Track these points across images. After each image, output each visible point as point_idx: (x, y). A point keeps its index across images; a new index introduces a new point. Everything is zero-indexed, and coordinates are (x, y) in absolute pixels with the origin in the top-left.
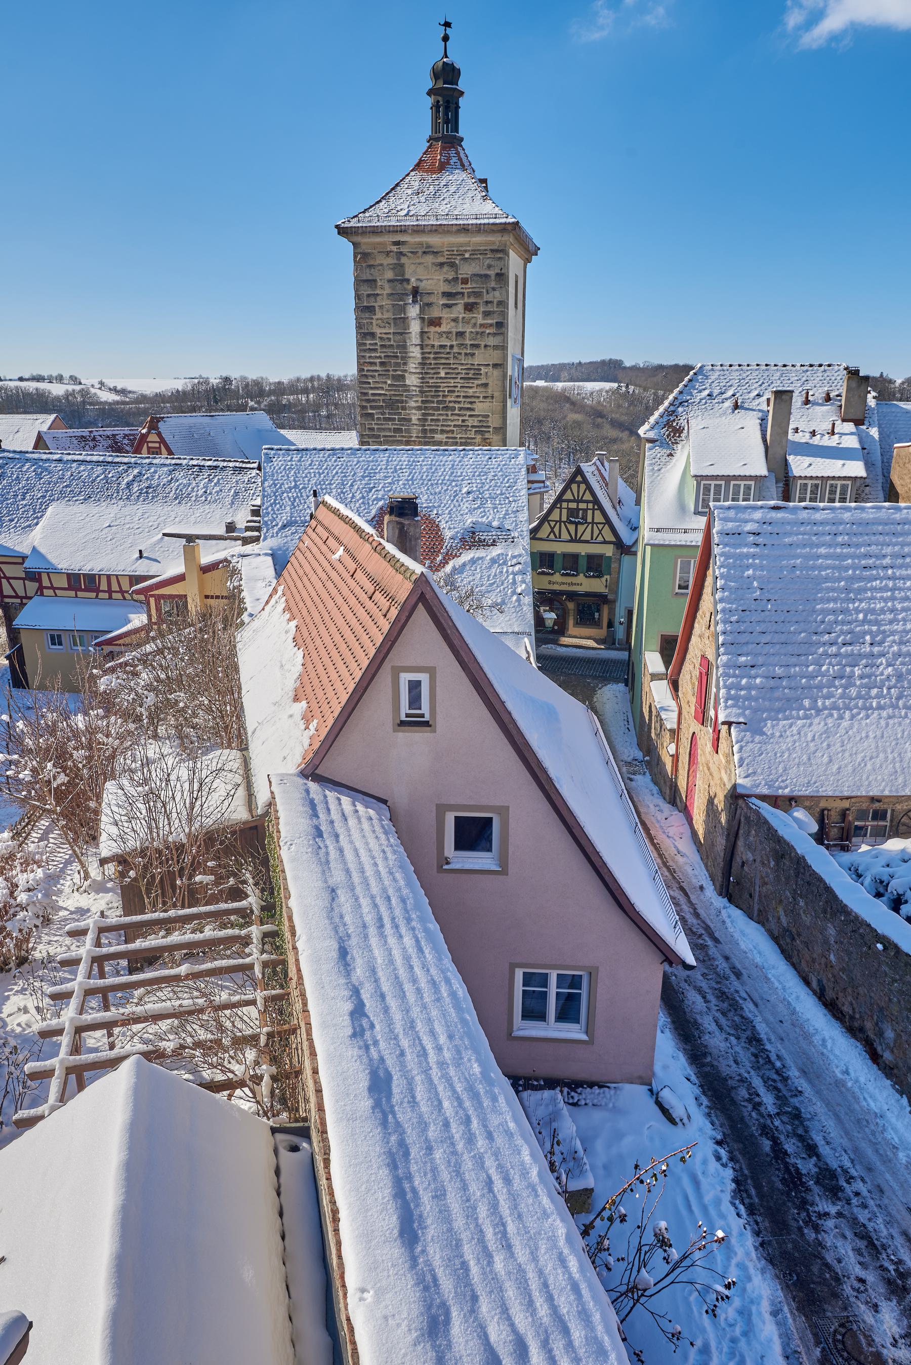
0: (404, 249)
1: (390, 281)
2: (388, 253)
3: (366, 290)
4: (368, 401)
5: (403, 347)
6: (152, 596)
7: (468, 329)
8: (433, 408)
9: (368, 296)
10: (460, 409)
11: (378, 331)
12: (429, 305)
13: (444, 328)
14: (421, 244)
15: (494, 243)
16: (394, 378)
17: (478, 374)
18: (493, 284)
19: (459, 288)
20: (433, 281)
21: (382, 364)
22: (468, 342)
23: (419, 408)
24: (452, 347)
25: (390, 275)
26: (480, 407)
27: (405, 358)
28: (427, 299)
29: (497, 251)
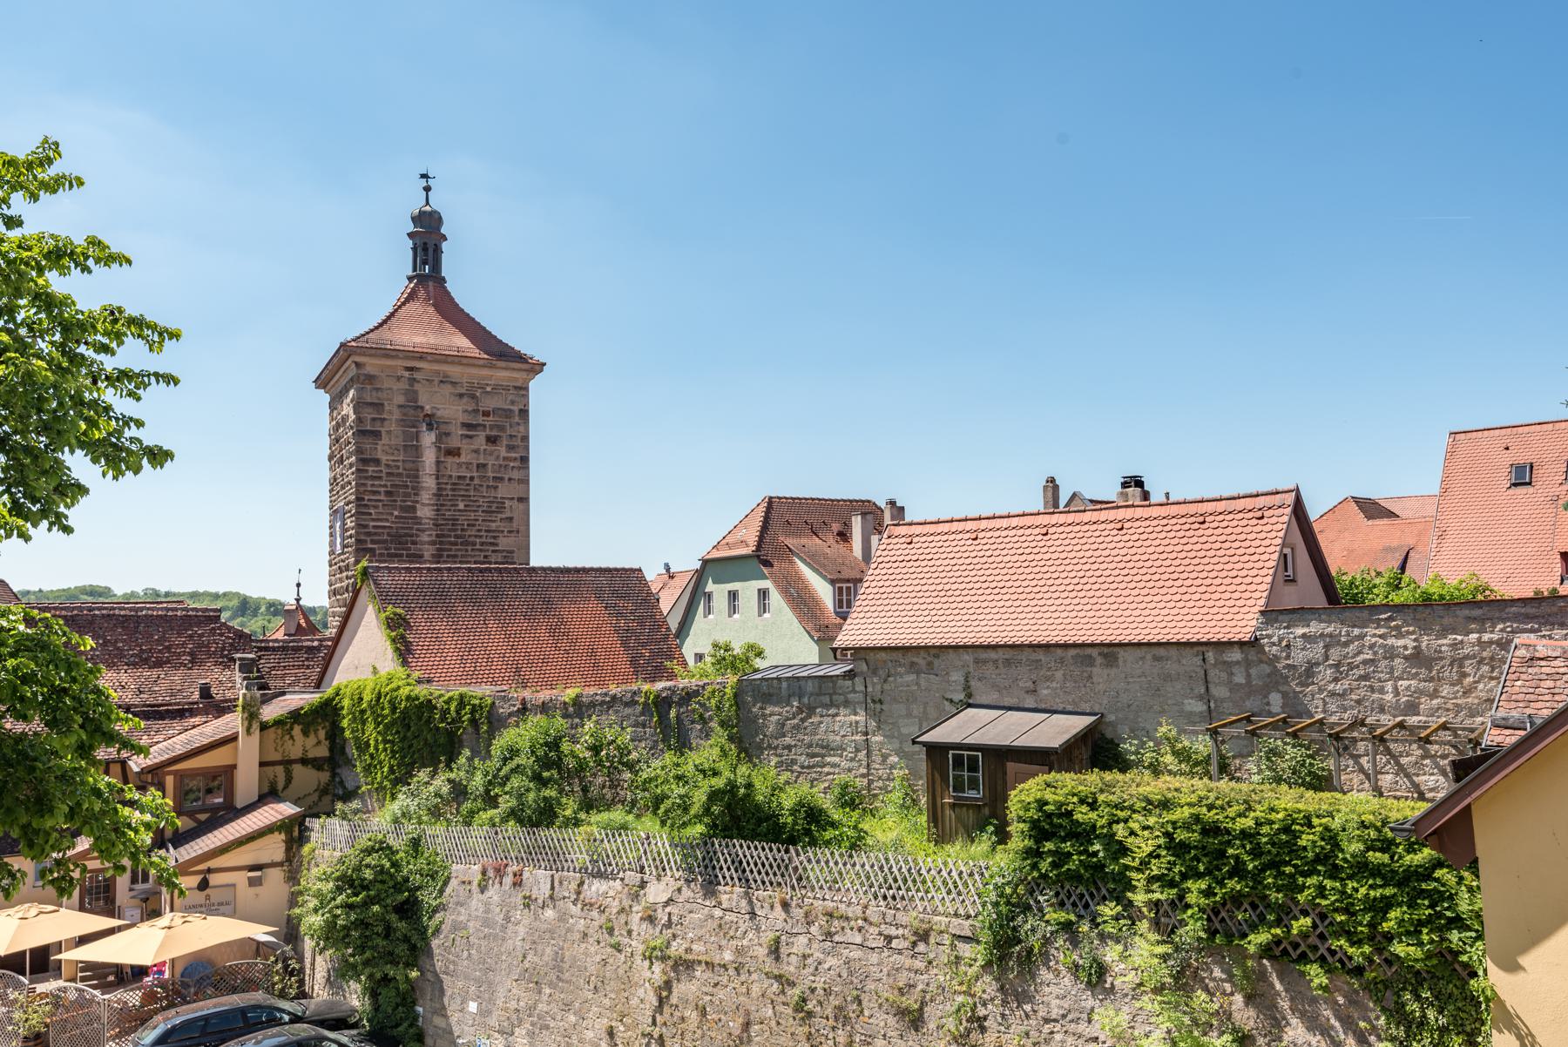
0: (417, 375)
1: (400, 406)
2: (399, 378)
3: (369, 414)
4: (369, 534)
5: (415, 476)
6: (170, 773)
7: (491, 462)
8: (452, 543)
9: (374, 419)
10: (482, 544)
11: (384, 458)
12: (447, 434)
13: (463, 459)
14: (438, 372)
15: (516, 379)
16: (402, 509)
17: (501, 508)
18: (517, 419)
19: (480, 419)
20: (452, 411)
21: (388, 493)
22: (491, 474)
23: (433, 543)
24: (472, 478)
25: (400, 400)
26: (504, 542)
27: (417, 490)
28: (444, 428)
29: (520, 388)
